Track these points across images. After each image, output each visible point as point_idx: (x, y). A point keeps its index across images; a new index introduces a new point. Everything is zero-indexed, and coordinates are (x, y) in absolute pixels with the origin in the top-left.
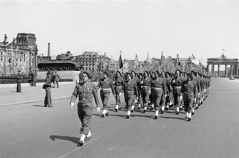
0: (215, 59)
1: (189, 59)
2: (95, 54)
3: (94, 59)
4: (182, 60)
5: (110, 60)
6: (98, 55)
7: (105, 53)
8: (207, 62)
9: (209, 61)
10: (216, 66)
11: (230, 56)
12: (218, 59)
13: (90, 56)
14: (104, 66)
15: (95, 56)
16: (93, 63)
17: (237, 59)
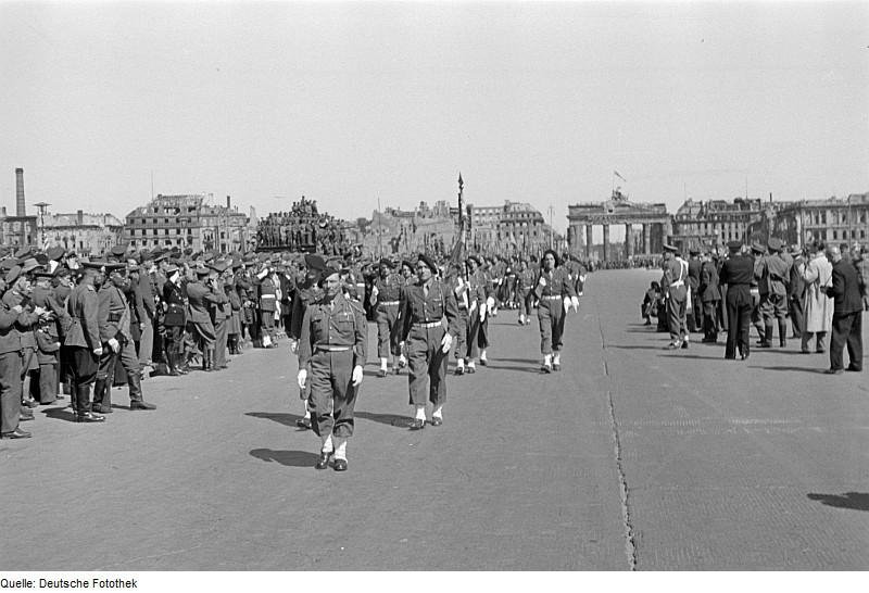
0: (592, 206)
1: (505, 208)
2: (193, 204)
3: (193, 220)
4: (484, 211)
5: (248, 220)
6: (206, 206)
7: (228, 198)
8: (568, 217)
9: (575, 212)
10: (597, 230)
11: (637, 196)
12: (600, 208)
13: (178, 210)
14: (228, 242)
15: (194, 209)
16: (190, 232)
17: (663, 205)
